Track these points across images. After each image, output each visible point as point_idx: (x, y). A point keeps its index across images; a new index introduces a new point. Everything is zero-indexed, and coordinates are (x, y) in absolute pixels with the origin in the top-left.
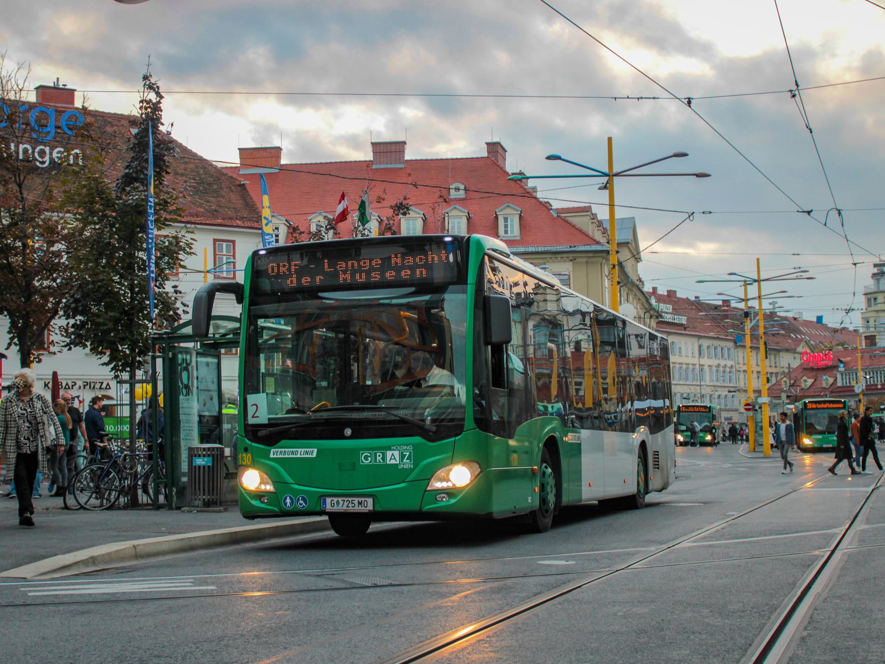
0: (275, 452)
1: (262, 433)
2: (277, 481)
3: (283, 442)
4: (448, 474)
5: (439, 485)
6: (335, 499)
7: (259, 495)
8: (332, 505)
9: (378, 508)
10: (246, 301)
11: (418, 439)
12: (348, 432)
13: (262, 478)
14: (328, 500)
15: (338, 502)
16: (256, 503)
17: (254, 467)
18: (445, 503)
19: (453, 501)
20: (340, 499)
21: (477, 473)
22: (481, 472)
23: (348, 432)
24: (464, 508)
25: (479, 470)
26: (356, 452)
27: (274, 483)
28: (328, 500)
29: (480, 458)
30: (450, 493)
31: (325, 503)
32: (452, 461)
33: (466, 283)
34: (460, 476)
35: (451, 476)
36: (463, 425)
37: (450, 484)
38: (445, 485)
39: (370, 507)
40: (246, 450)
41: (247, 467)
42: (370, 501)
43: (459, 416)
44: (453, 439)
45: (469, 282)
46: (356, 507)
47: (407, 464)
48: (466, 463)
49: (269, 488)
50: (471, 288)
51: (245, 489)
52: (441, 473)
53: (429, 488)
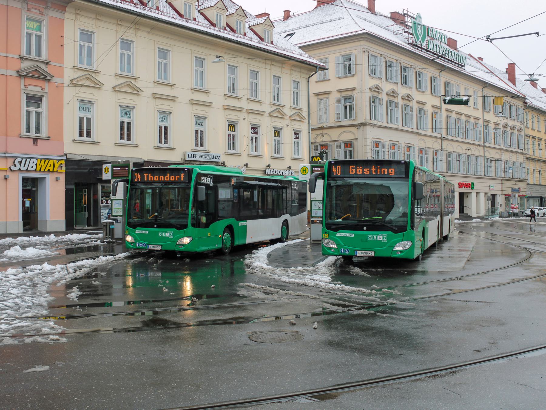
0: (338, 234)
1: (333, 227)
3: (340, 231)
9: (376, 256)
10: (326, 179)
12: (365, 228)
14: (358, 252)
26: (367, 235)
27: (337, 245)
39: (373, 255)
40: (326, 233)
42: (373, 252)
47: (385, 240)
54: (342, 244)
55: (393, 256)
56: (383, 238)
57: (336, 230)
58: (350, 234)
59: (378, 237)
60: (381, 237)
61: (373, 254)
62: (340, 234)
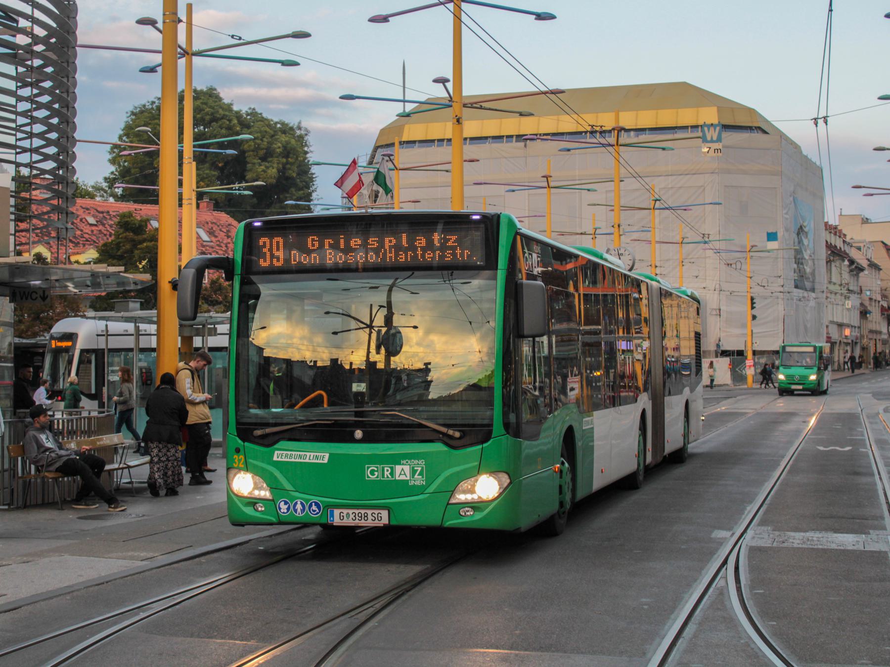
1: (258, 432)
2: (274, 487)
3: (282, 444)
4: (473, 486)
5: (462, 497)
6: (345, 511)
7: (253, 502)
8: (341, 518)
9: (394, 523)
11: (438, 447)
12: (359, 434)
13: (255, 483)
14: (337, 512)
15: (348, 513)
16: (249, 511)
17: (247, 470)
18: (470, 518)
19: (478, 516)
20: (351, 511)
21: (505, 485)
22: (510, 483)
23: (359, 434)
24: (494, 524)
25: (508, 481)
27: (272, 489)
28: (337, 512)
29: (512, 470)
30: (476, 506)
31: (332, 515)
32: (478, 472)
33: (496, 269)
34: (487, 487)
35: (477, 489)
36: (490, 432)
37: (475, 497)
38: (469, 497)
39: (385, 521)
40: (238, 451)
41: (240, 470)
42: (385, 514)
43: (486, 422)
44: (480, 447)
45: (499, 267)
46: (370, 521)
48: (493, 473)
49: (265, 494)
50: (501, 274)
51: (237, 495)
52: (465, 485)
53: (453, 501)
54: (288, 486)
55: (451, 522)
56: (413, 472)
57: (268, 441)
58: (316, 454)
59: (398, 468)
60: (407, 469)
61: (384, 518)
62: (287, 453)
